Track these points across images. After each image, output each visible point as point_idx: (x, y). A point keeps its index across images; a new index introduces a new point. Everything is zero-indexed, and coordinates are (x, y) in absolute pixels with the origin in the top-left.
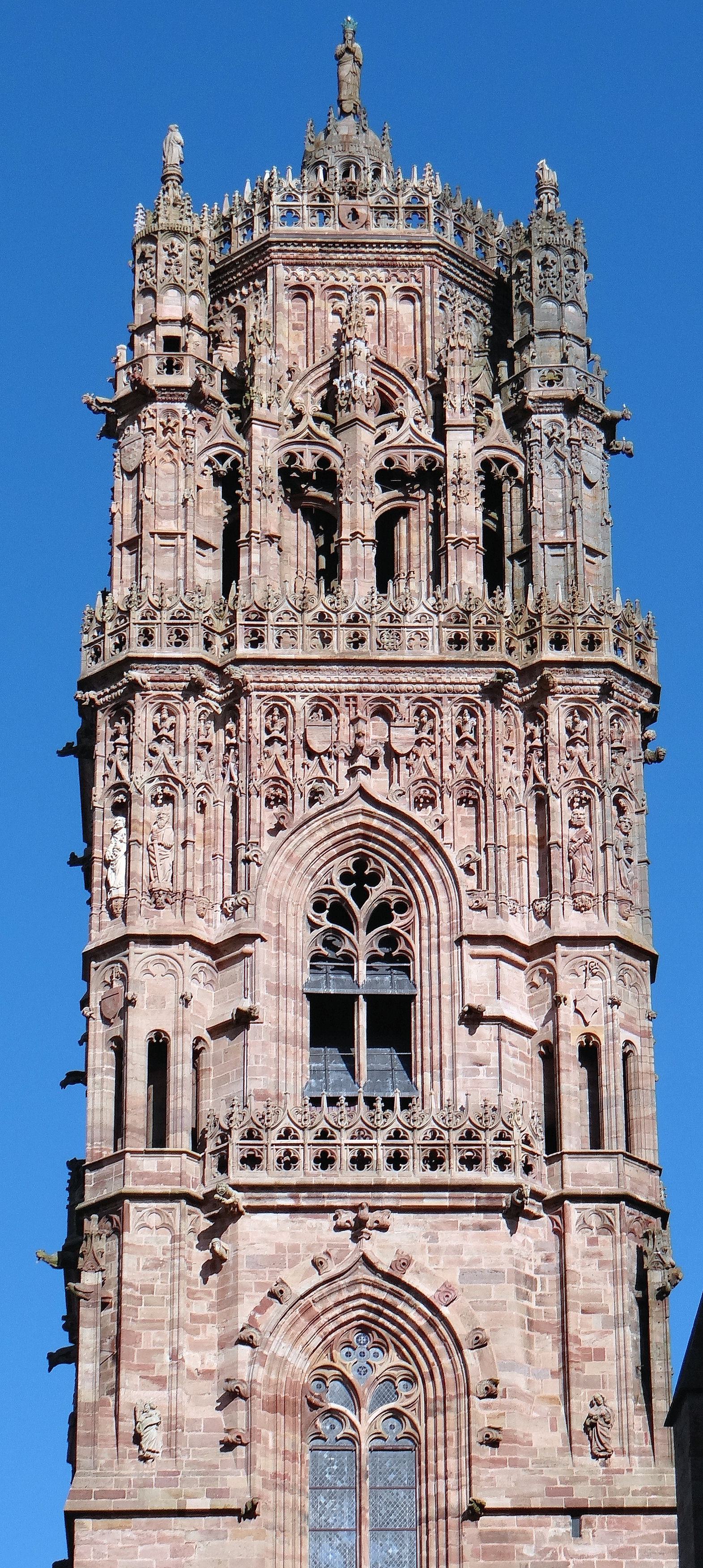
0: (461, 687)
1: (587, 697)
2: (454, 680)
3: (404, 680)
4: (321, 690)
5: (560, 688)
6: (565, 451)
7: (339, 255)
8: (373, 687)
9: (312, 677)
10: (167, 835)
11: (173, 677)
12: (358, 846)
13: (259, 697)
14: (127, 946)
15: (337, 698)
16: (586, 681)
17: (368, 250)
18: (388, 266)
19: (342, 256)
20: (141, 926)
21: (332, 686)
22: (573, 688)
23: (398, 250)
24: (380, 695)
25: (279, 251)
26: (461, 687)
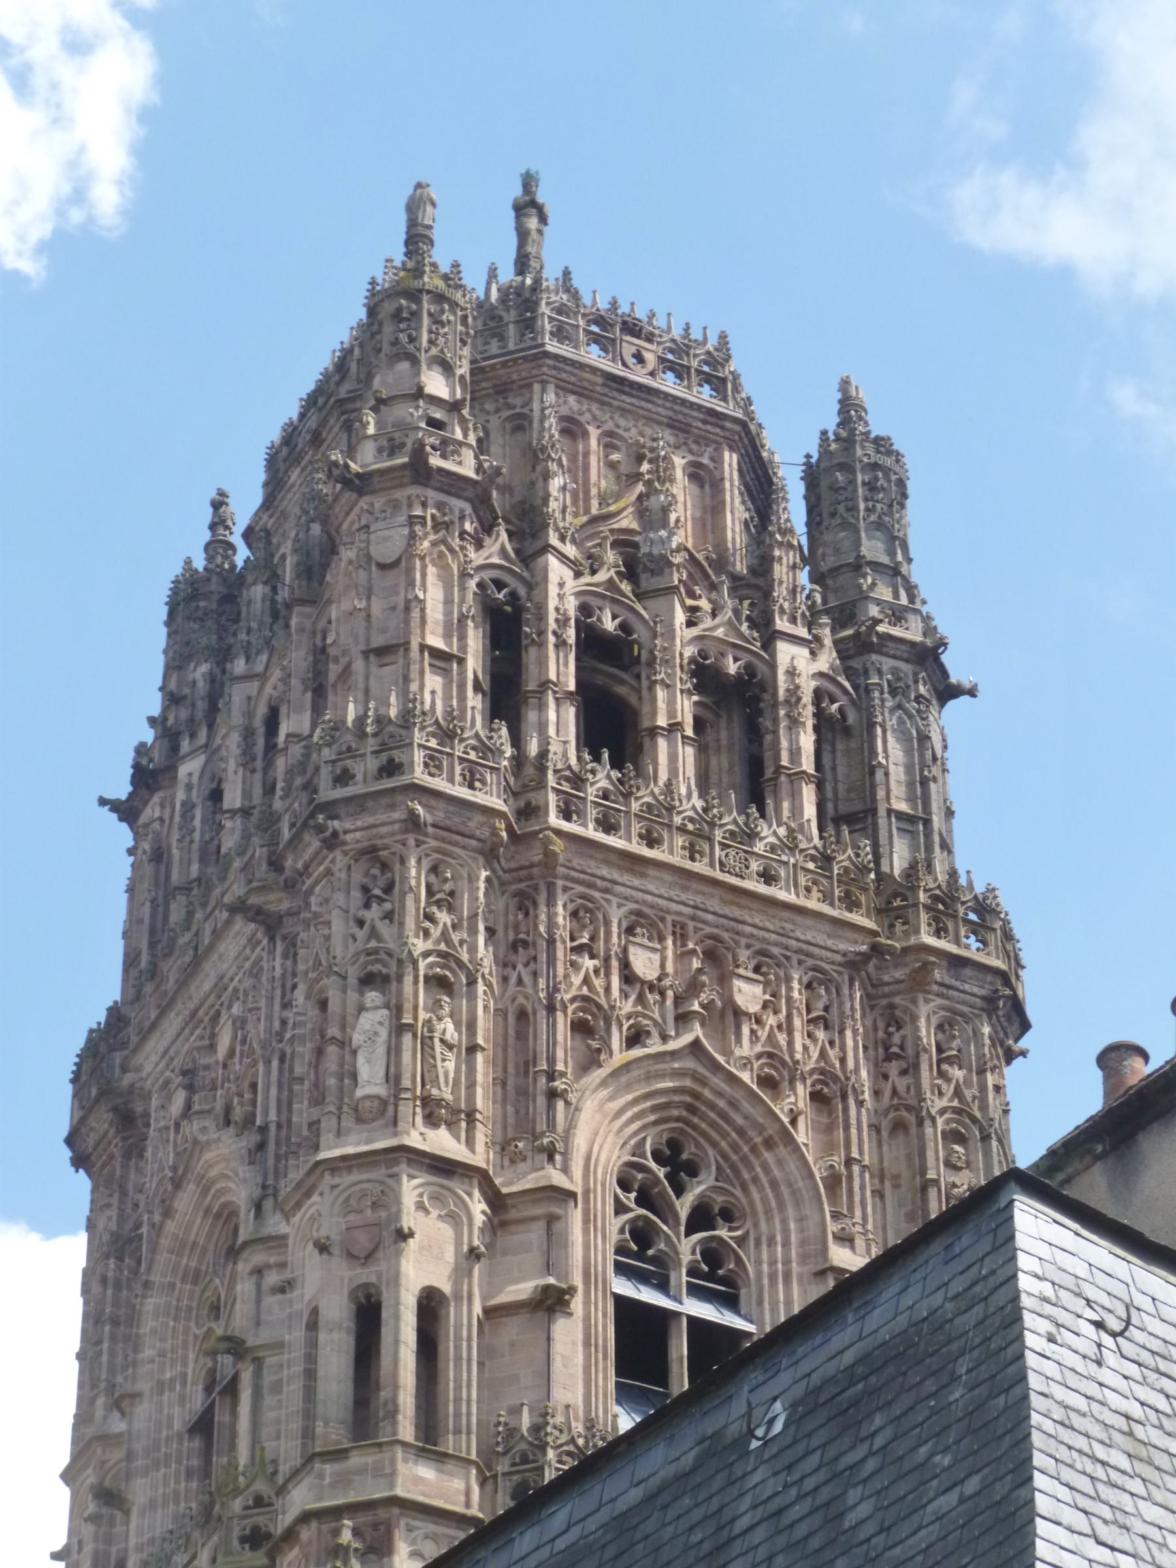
0: (816, 951)
1: (965, 1009)
2: (809, 938)
3: (750, 920)
4: (645, 903)
5: (935, 988)
6: (912, 706)
7: (624, 397)
8: (710, 917)
9: (636, 882)
10: (448, 1028)
11: (461, 828)
12: (678, 1119)
13: (565, 889)
14: (396, 1162)
15: (662, 919)
16: (967, 987)
17: (660, 402)
18: (679, 429)
19: (629, 400)
20: (413, 1139)
21: (660, 901)
22: (951, 992)
23: (695, 414)
24: (716, 931)
25: (555, 368)
26: (816, 951)
